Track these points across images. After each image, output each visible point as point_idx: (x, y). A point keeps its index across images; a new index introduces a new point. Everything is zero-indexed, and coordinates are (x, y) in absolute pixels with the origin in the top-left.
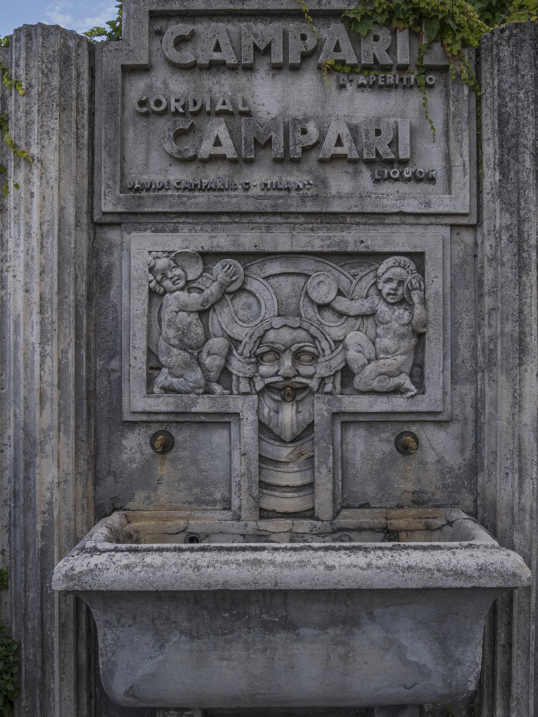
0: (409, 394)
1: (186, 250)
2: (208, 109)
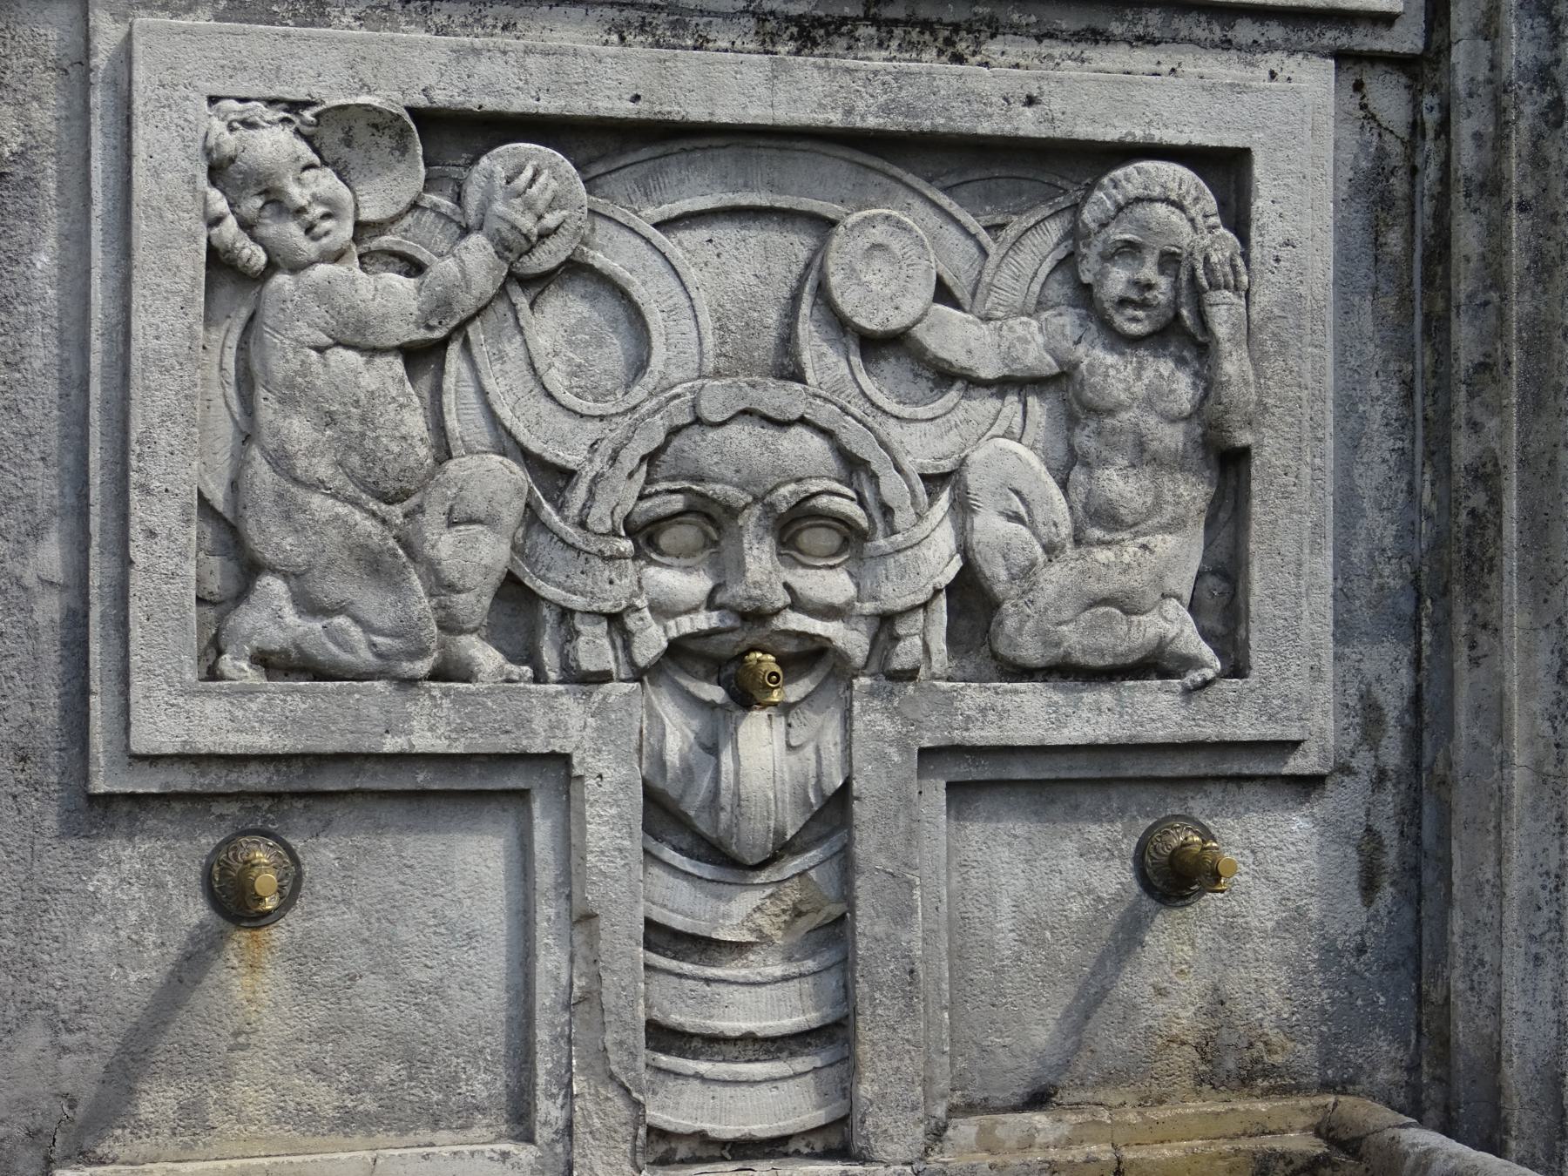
0: (1195, 676)
1: (363, 99)
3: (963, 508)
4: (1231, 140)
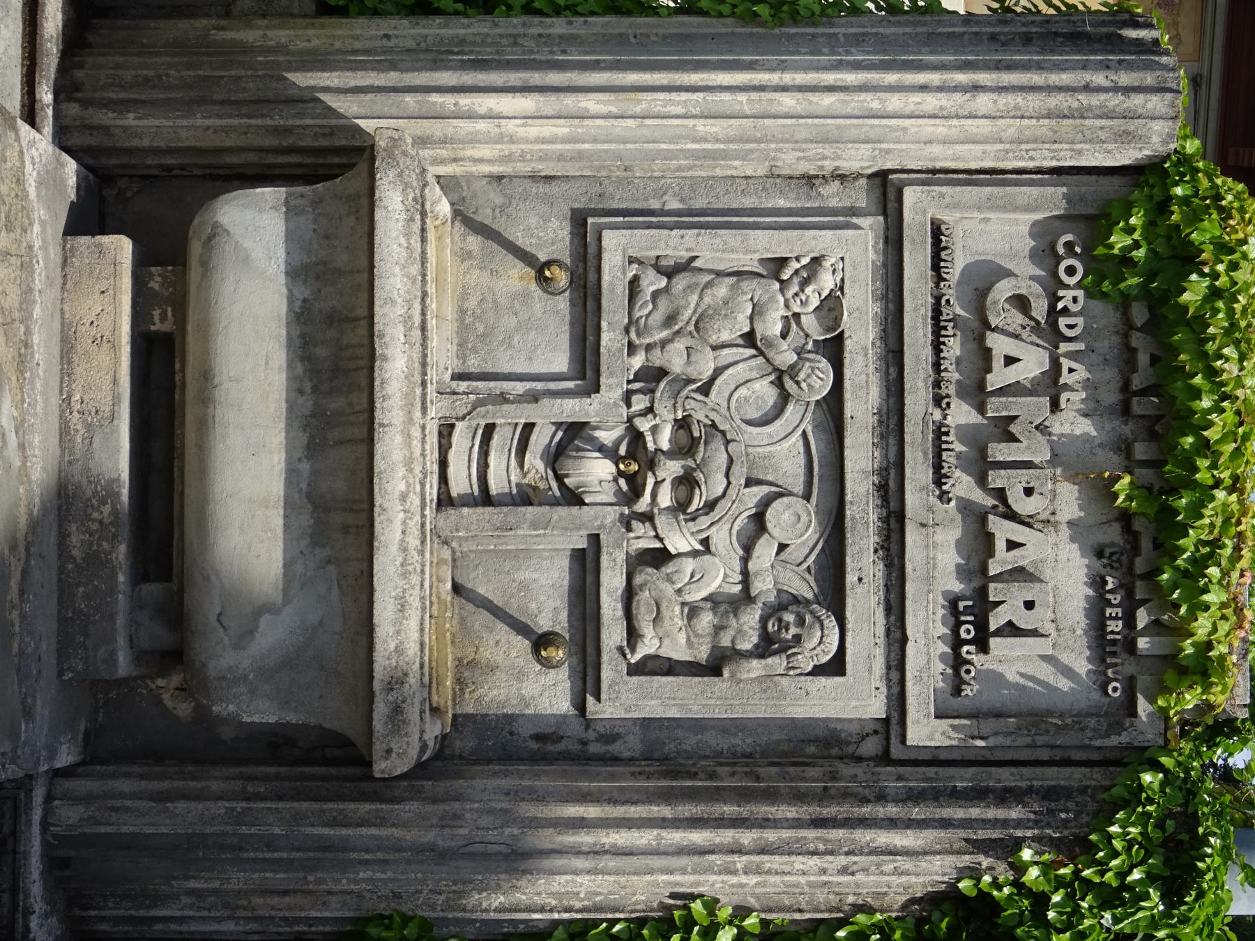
0: (627, 651)
2: (1064, 347)
3: (694, 554)
4: (849, 667)
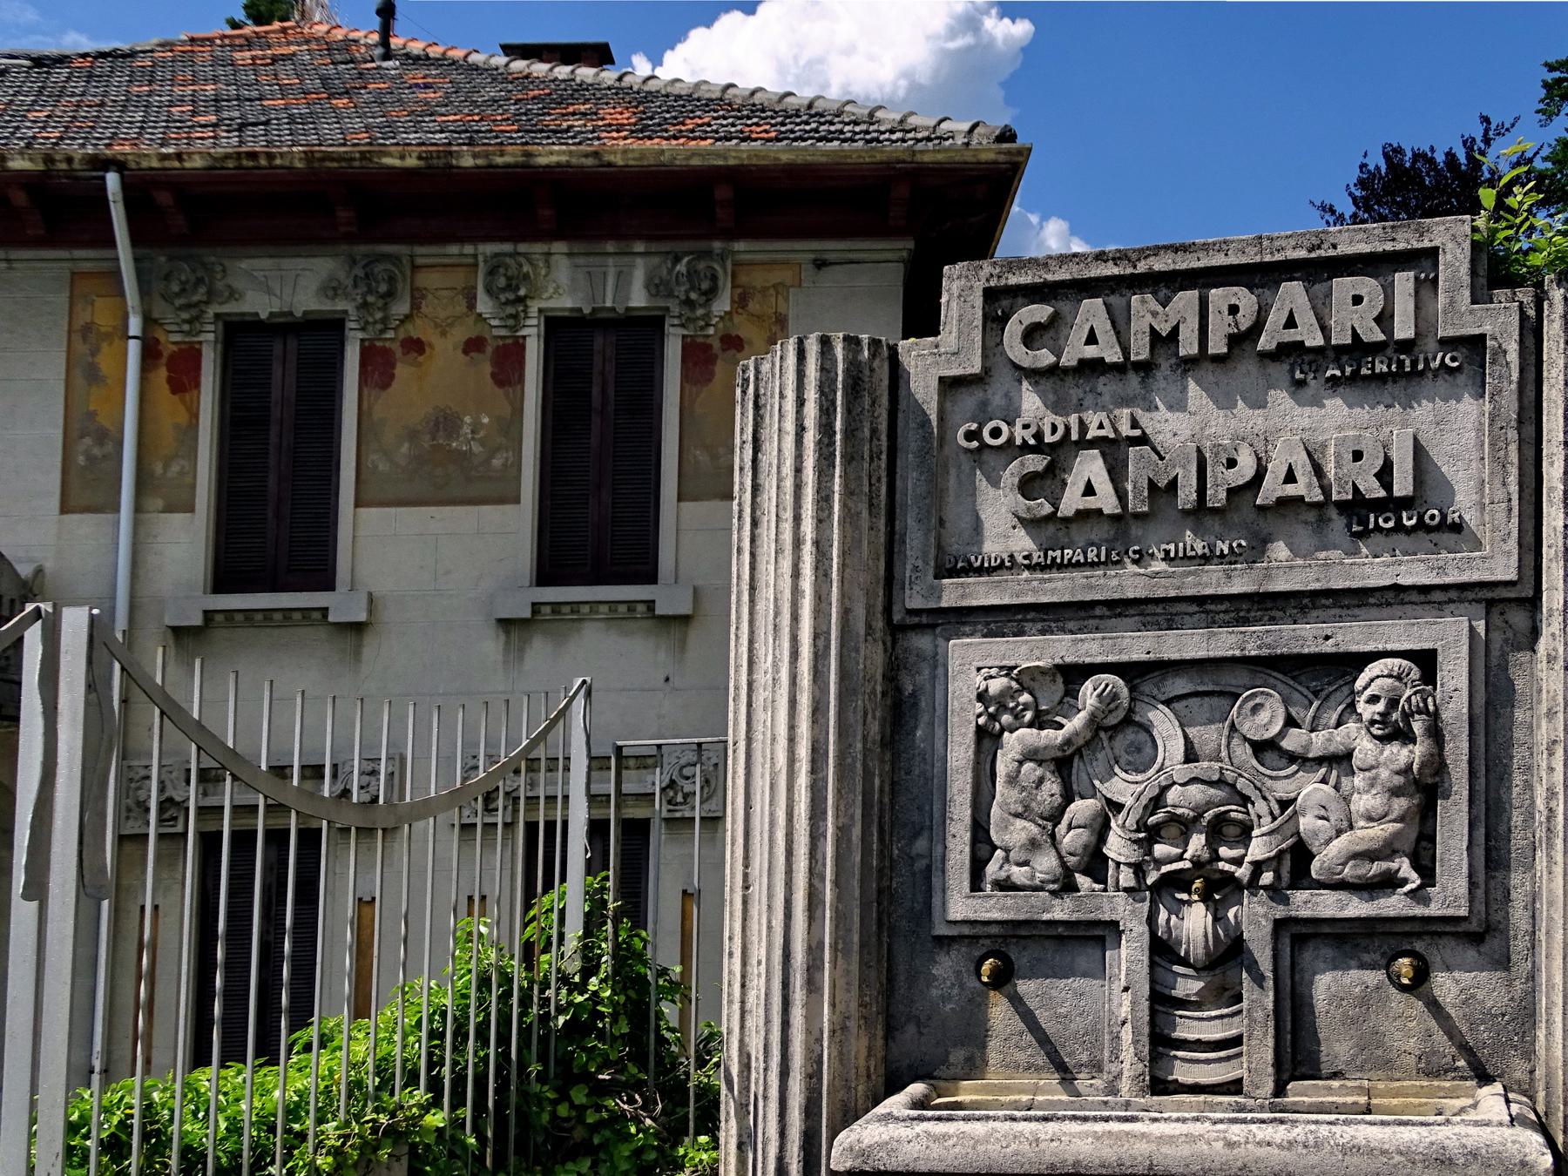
0: (1408, 887)
2: (1074, 436)
4: (1426, 646)
